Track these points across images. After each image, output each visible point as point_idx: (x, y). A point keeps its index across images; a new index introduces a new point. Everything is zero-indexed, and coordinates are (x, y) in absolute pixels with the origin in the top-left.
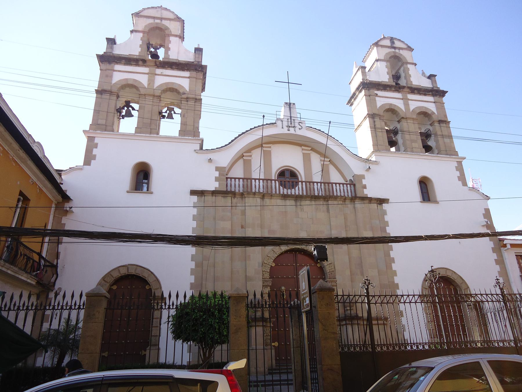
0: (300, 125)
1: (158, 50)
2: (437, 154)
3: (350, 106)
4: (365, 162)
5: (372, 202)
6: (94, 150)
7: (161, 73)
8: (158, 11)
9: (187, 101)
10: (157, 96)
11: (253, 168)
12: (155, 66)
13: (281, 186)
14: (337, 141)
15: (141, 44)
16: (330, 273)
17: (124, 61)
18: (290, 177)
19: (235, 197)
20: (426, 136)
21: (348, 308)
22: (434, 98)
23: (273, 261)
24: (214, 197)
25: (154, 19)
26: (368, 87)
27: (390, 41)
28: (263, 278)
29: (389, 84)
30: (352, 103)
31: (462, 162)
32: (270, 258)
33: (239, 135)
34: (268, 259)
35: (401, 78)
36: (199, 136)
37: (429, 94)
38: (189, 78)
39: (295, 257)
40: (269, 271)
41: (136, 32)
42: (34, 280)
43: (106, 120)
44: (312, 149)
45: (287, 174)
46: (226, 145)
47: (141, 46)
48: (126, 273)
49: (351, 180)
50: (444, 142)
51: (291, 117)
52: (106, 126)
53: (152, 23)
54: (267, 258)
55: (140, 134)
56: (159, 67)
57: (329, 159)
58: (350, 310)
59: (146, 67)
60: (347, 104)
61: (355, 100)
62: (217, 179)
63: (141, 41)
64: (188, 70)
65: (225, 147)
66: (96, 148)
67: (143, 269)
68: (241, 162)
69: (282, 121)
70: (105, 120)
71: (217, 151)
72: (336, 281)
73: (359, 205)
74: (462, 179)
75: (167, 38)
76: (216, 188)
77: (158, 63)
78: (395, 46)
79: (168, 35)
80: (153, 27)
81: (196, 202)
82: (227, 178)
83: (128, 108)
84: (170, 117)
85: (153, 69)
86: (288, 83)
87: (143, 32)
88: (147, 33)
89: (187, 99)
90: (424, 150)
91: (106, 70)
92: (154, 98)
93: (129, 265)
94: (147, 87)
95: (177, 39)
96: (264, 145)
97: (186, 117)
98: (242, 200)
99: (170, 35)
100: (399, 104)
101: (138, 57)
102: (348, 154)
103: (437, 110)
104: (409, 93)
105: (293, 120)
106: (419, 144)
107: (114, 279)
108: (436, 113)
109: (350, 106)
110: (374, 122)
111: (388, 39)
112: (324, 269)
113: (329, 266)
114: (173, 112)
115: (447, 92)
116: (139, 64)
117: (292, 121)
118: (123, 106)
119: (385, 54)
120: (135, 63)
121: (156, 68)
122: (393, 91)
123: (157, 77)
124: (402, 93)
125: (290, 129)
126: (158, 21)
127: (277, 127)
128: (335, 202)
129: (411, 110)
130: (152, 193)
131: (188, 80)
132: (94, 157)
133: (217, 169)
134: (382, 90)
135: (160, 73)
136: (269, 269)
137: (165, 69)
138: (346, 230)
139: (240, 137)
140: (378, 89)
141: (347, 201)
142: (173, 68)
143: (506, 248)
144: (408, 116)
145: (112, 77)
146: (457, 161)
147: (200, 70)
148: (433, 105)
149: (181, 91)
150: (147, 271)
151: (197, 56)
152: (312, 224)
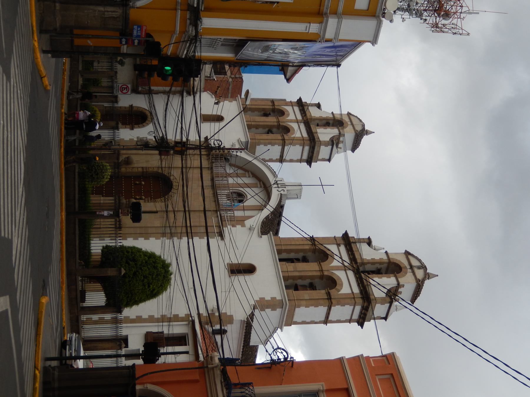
12: (305, 121)
19: (207, 156)
27: (420, 266)
28: (148, 167)
38: (302, 136)
43: (251, 105)
51: (286, 186)
72: (149, 202)
78: (416, 270)
86: (322, 185)
95: (338, 132)
104: (353, 271)
108: (339, 293)
117: (285, 186)
126: (349, 123)
131: (300, 136)
140: (346, 246)
146: (282, 300)
149: (289, 134)
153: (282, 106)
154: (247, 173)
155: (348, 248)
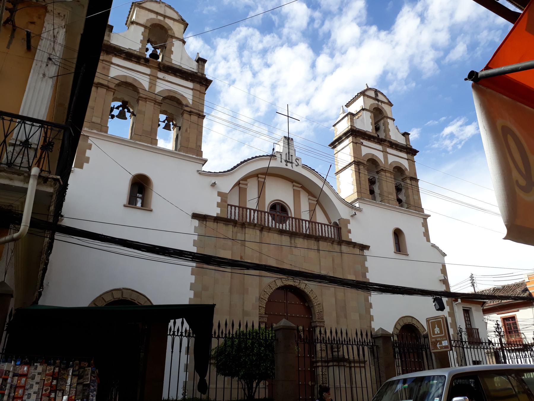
0: (297, 162)
1: (157, 50)
2: (407, 208)
3: (332, 148)
4: (352, 209)
5: (356, 247)
6: (88, 151)
7: (163, 77)
8: (161, 6)
9: (190, 115)
10: (159, 103)
11: (248, 198)
12: (158, 68)
13: (273, 221)
14: (328, 183)
15: (142, 39)
16: (319, 313)
17: (125, 55)
18: (280, 212)
19: (235, 226)
20: (398, 189)
21: (336, 350)
22: (407, 155)
23: (268, 296)
24: (216, 223)
25: (157, 14)
26: (355, 135)
27: (375, 92)
29: (372, 134)
30: (336, 145)
31: (427, 219)
32: (267, 293)
33: (242, 163)
34: (265, 294)
35: (380, 130)
36: (201, 156)
37: (404, 151)
39: (286, 295)
40: (265, 307)
43: (101, 119)
44: (303, 187)
45: (278, 208)
46: (228, 171)
47: (141, 41)
48: (120, 298)
49: (335, 223)
50: (414, 199)
51: (289, 153)
52: (102, 125)
53: (154, 19)
54: (264, 293)
55: (140, 142)
56: (162, 70)
57: (317, 199)
58: (338, 351)
59: (147, 67)
60: (329, 146)
61: (339, 143)
62: (219, 205)
63: (142, 36)
64: (192, 81)
65: (228, 172)
66: (90, 149)
67: (139, 294)
68: (237, 188)
69: (281, 155)
70: (100, 119)
71: (220, 175)
72: (324, 322)
73: (344, 248)
74: (426, 234)
75: (169, 39)
76: (217, 214)
77: (161, 66)
79: (172, 36)
80: (155, 24)
81: (197, 227)
82: (228, 205)
83: (123, 109)
84: (167, 127)
85: (155, 71)
89: (190, 113)
90: (398, 203)
92: (156, 104)
93: (124, 289)
94: (147, 90)
95: (181, 43)
96: (259, 176)
97: (189, 132)
98: (242, 230)
99: (174, 37)
100: (380, 156)
101: (138, 54)
102: (337, 197)
103: (409, 166)
104: (388, 147)
105: (291, 155)
106: (394, 196)
107: (107, 303)
108: (409, 170)
109: (332, 148)
110: (359, 169)
111: (373, 90)
112: (312, 309)
113: (318, 306)
114: (171, 123)
115: (419, 151)
116: (141, 62)
117: (290, 156)
118: (119, 106)
119: (370, 105)
121: (159, 71)
122: (376, 142)
123: (158, 80)
124: (382, 146)
125: (288, 164)
127: (276, 160)
128: (325, 243)
129: (389, 164)
130: (151, 211)
131: (191, 92)
132: (87, 160)
133: (220, 194)
134: (366, 140)
135: (162, 77)
136: (265, 304)
137: (168, 74)
138: (333, 272)
139: (242, 165)
140: (364, 139)
141: (334, 243)
142: (177, 75)
143: (457, 302)
144: (388, 168)
146: (423, 218)
147: (204, 83)
148: (407, 161)
149: (184, 102)
150: (143, 297)
151: (200, 67)
152: (305, 262)
154: (241, 185)
155: (367, 138)
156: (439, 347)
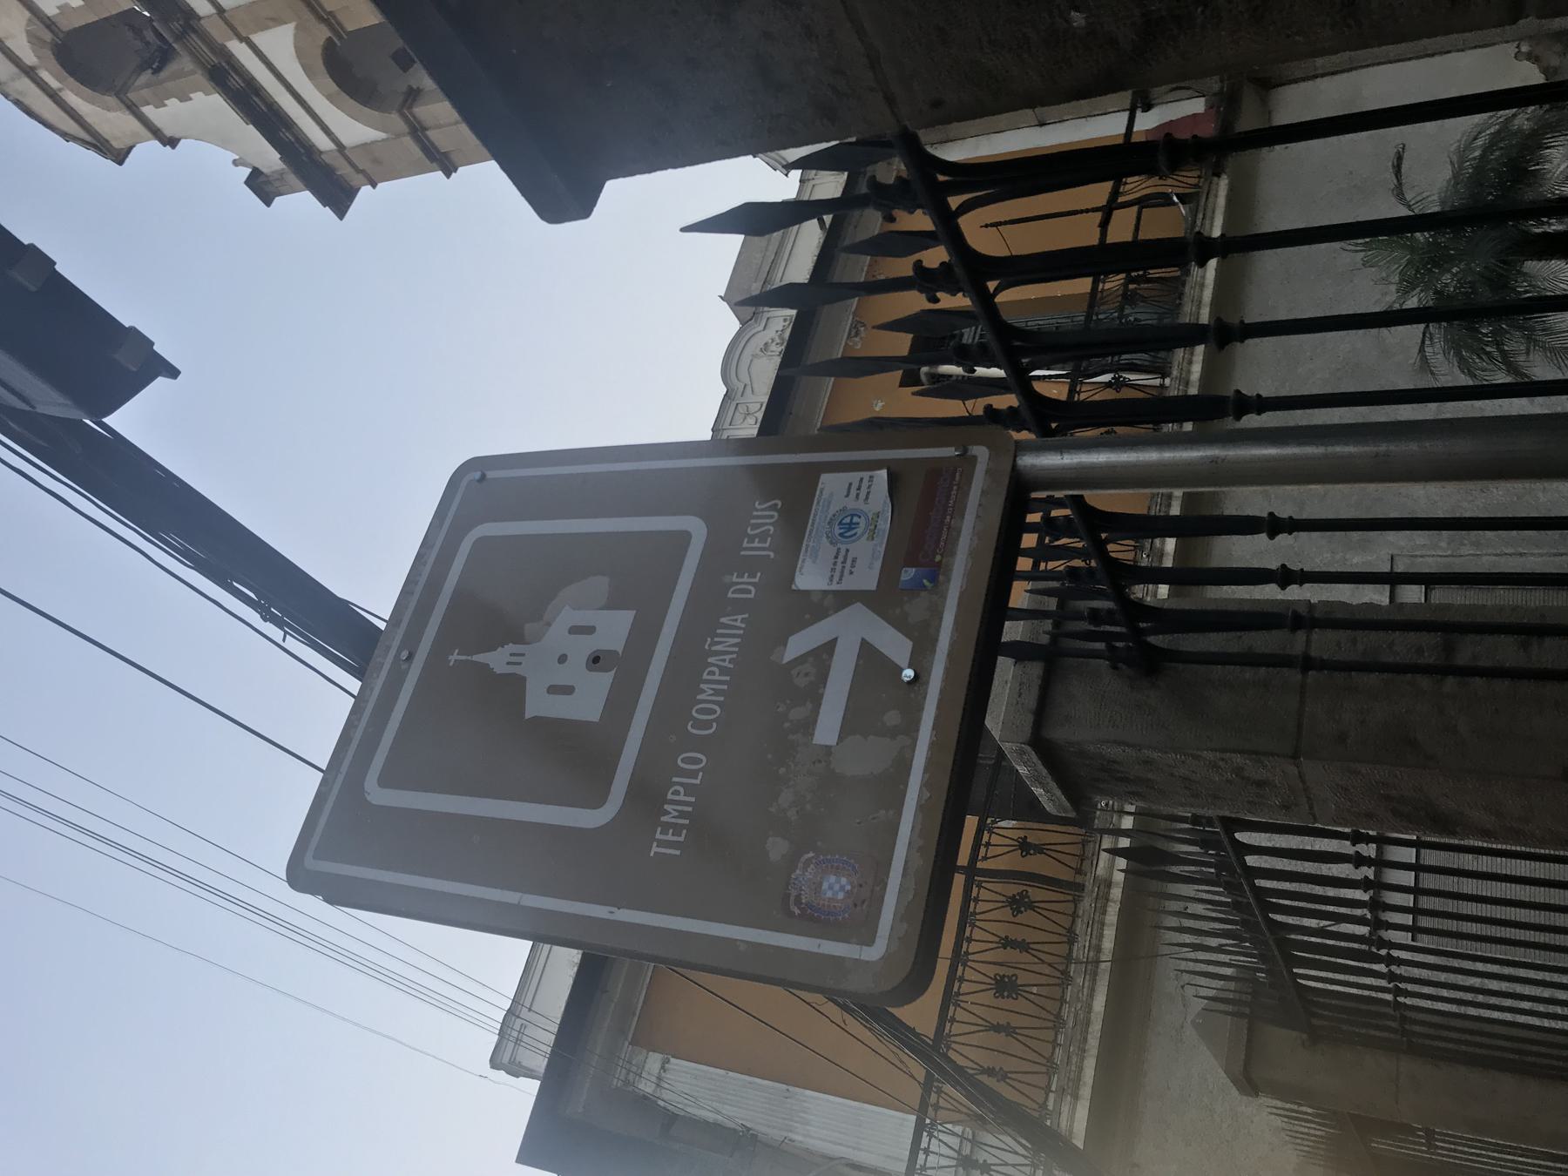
12: (195, 31)
17: (281, 134)
41: (159, 130)
42: (1211, 199)
47: (184, 98)
75: (67, 25)
77: (176, 26)
79: (48, 27)
85: (216, 30)
87: (133, 109)
88: (122, 96)
91: (362, 172)
120: (255, 98)
121: (200, 18)
126: (45, 75)
145: (366, 144)
153: (380, 135)
156: (830, 647)
